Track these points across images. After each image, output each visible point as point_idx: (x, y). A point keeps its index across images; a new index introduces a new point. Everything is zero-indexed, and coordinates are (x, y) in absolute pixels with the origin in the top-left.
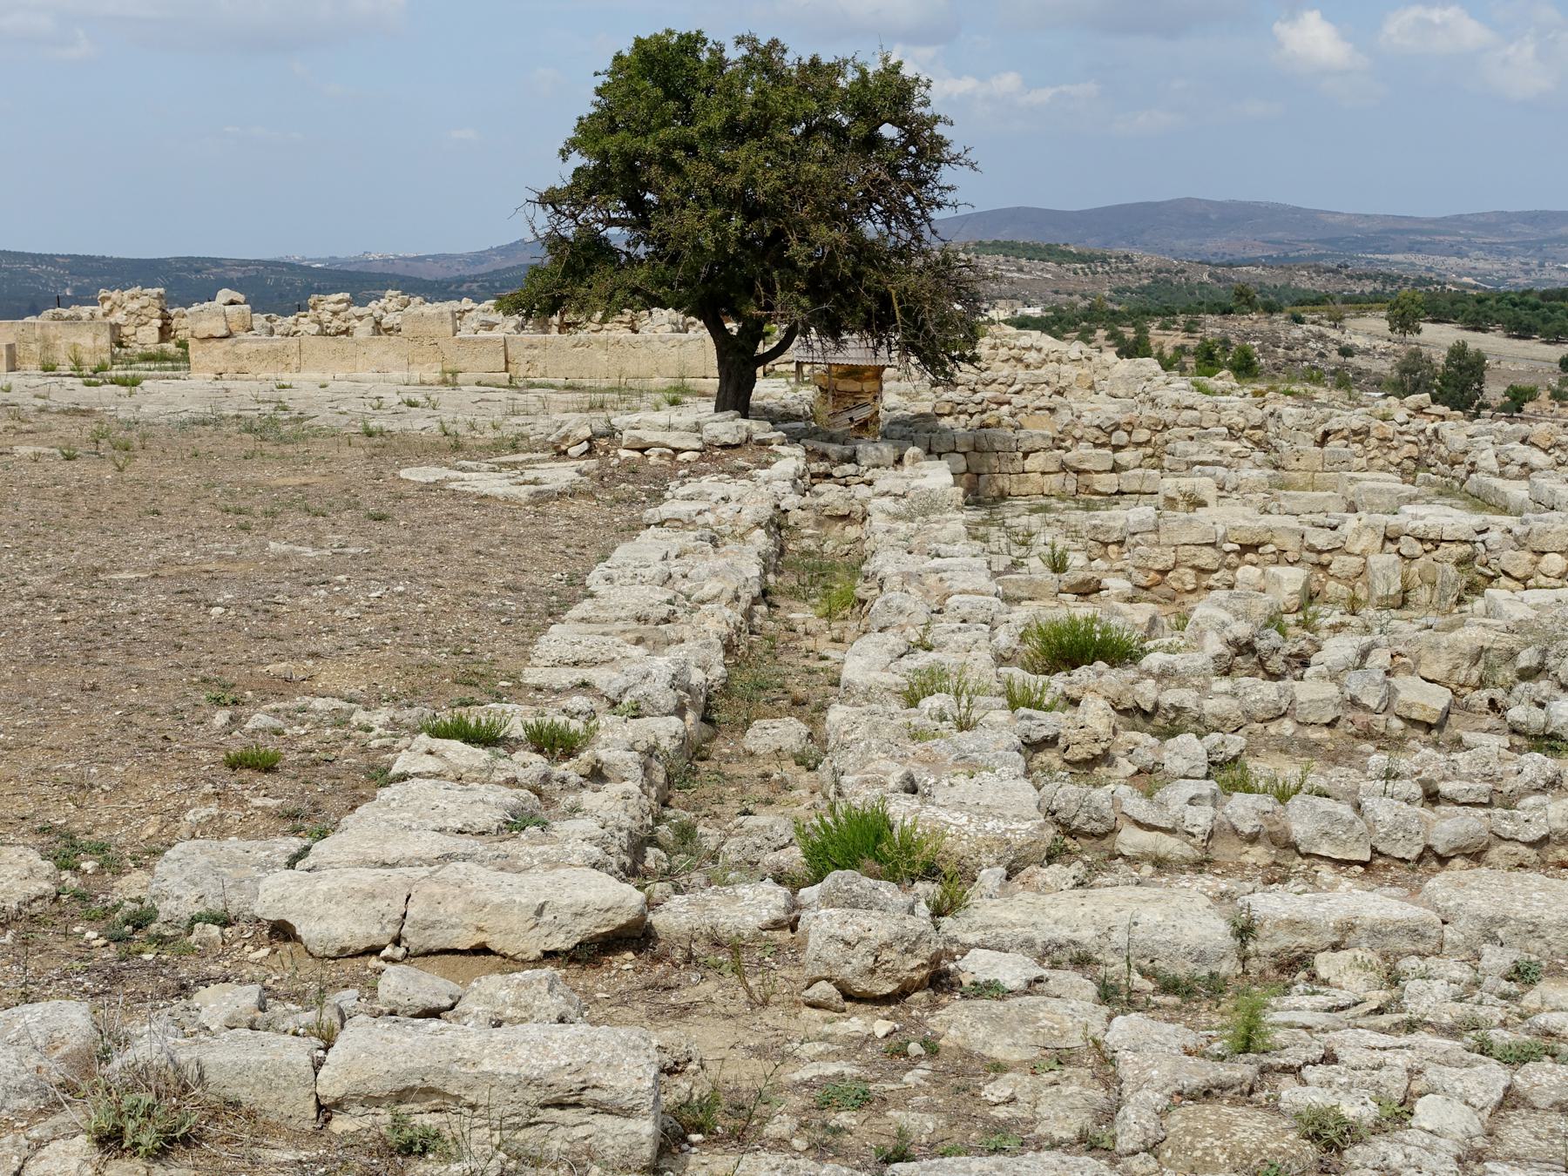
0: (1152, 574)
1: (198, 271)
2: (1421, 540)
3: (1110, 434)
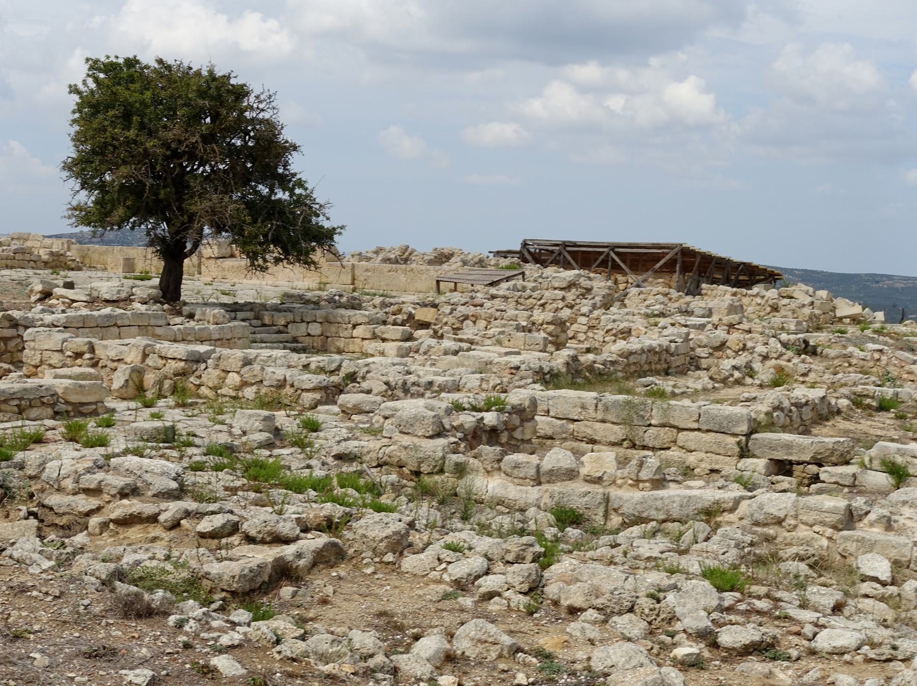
0: (31, 368)
1: (877, 282)
2: (162, 357)
3: (462, 322)
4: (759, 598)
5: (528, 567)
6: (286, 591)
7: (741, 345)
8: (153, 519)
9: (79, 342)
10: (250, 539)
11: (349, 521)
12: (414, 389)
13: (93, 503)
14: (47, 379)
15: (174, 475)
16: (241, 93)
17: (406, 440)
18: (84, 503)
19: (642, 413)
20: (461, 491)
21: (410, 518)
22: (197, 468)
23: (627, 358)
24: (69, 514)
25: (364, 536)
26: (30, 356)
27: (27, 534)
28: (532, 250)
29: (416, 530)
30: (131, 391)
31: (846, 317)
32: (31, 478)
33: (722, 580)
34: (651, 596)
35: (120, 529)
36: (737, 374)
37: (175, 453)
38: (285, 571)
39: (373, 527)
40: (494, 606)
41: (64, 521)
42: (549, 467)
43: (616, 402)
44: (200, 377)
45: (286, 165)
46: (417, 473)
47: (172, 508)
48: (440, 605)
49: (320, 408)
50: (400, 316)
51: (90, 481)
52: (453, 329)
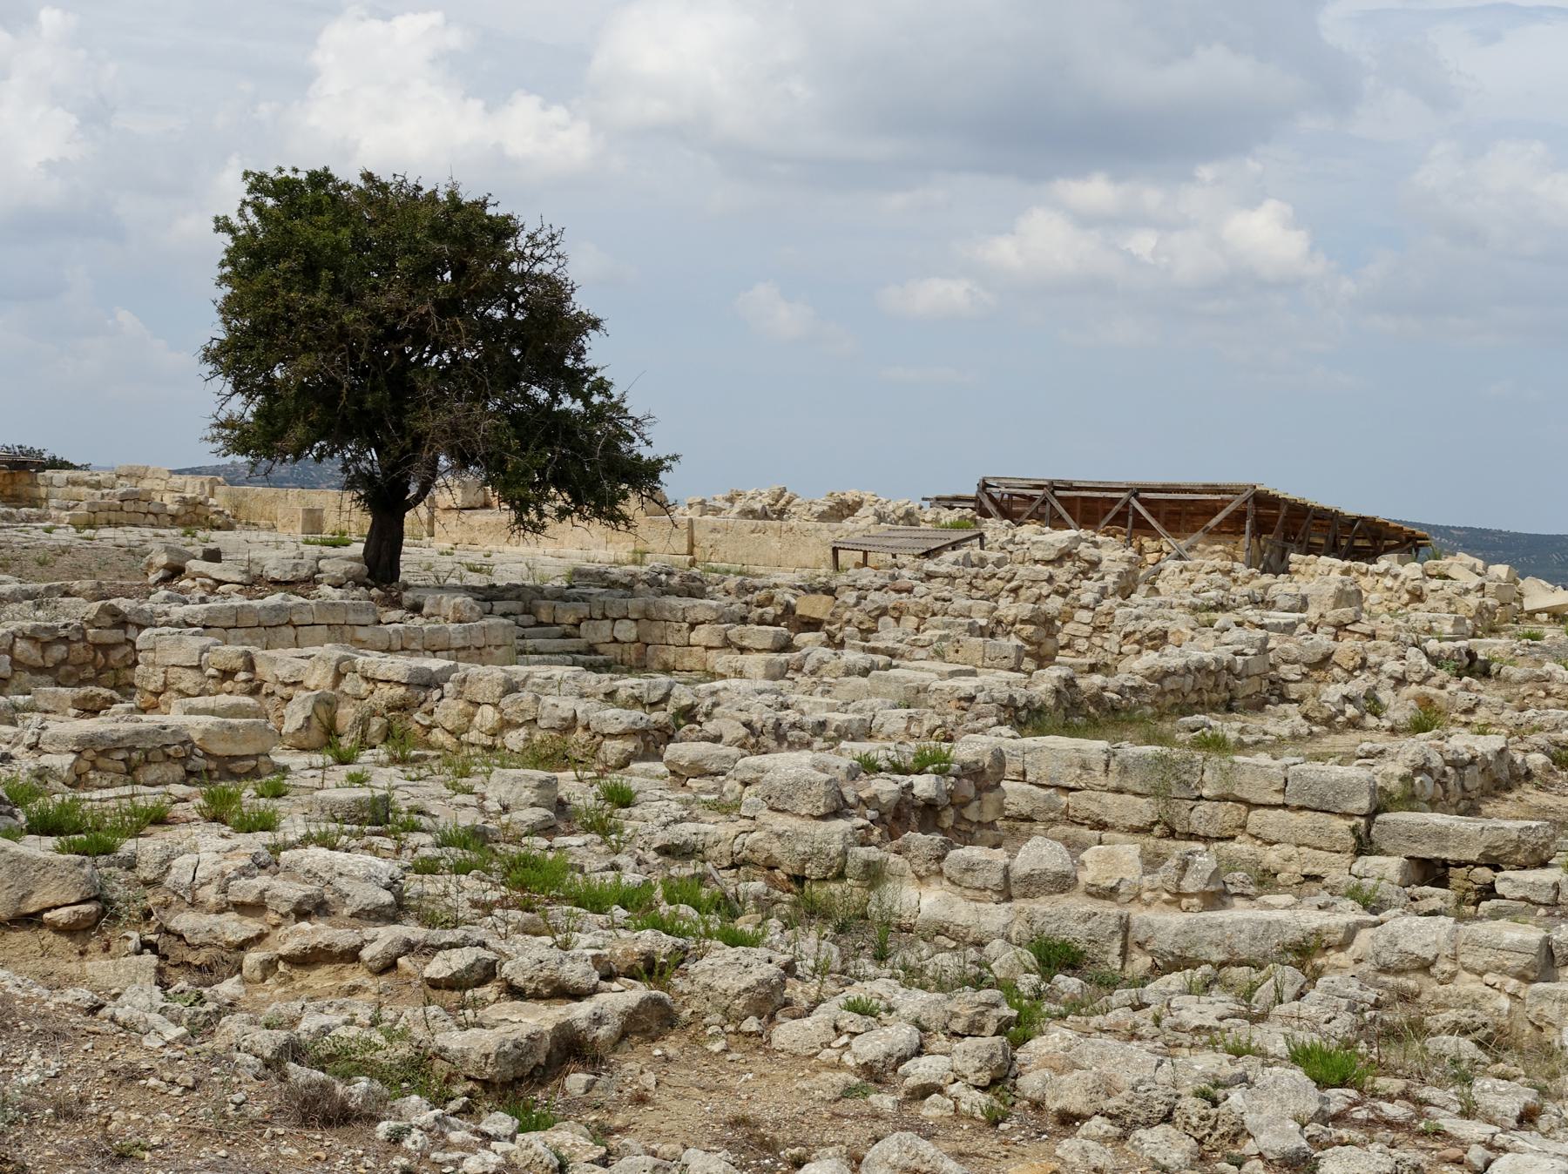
0: (147, 695)
2: (367, 679)
3: (876, 619)
4: (1390, 1098)
5: (989, 1042)
6: (576, 1081)
7: (1358, 660)
8: (351, 955)
9: (229, 653)
10: (514, 992)
11: (682, 961)
12: (793, 735)
13: (251, 926)
14: (174, 716)
15: (386, 880)
16: (504, 229)
17: (781, 823)
18: (235, 927)
19: (1185, 777)
20: (872, 908)
21: (787, 957)
22: (428, 868)
23: (1159, 681)
24: (210, 945)
25: (709, 987)
26: (147, 676)
27: (139, 979)
28: (997, 496)
29: (798, 977)
30: (315, 736)
31: (1540, 611)
32: (147, 883)
33: (1325, 1068)
34: (1202, 1094)
35: (296, 973)
36: (1351, 710)
37: (389, 843)
38: (571, 1048)
39: (725, 971)
40: (932, 1109)
41: (202, 957)
42: (1026, 869)
43: (1140, 758)
44: (431, 712)
45: (579, 353)
46: (799, 879)
47: (383, 938)
48: (839, 1108)
49: (635, 766)
50: (770, 609)
51: (245, 890)
52: (861, 631)
